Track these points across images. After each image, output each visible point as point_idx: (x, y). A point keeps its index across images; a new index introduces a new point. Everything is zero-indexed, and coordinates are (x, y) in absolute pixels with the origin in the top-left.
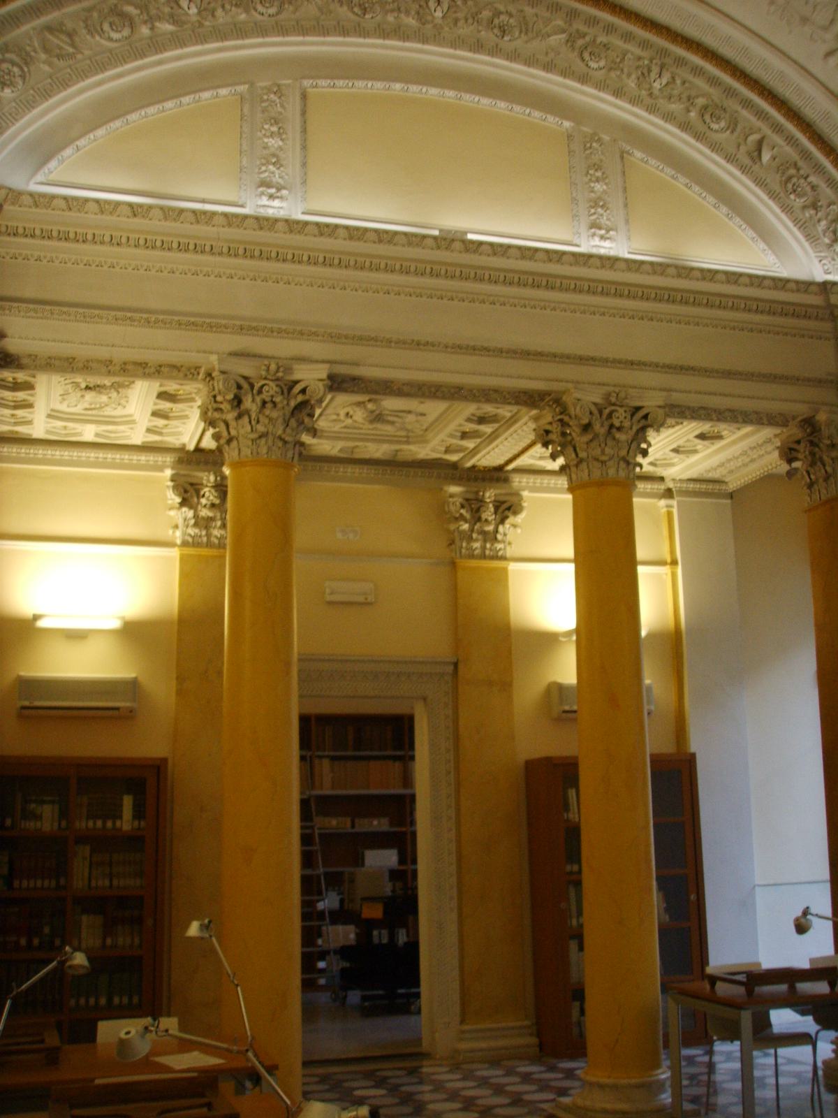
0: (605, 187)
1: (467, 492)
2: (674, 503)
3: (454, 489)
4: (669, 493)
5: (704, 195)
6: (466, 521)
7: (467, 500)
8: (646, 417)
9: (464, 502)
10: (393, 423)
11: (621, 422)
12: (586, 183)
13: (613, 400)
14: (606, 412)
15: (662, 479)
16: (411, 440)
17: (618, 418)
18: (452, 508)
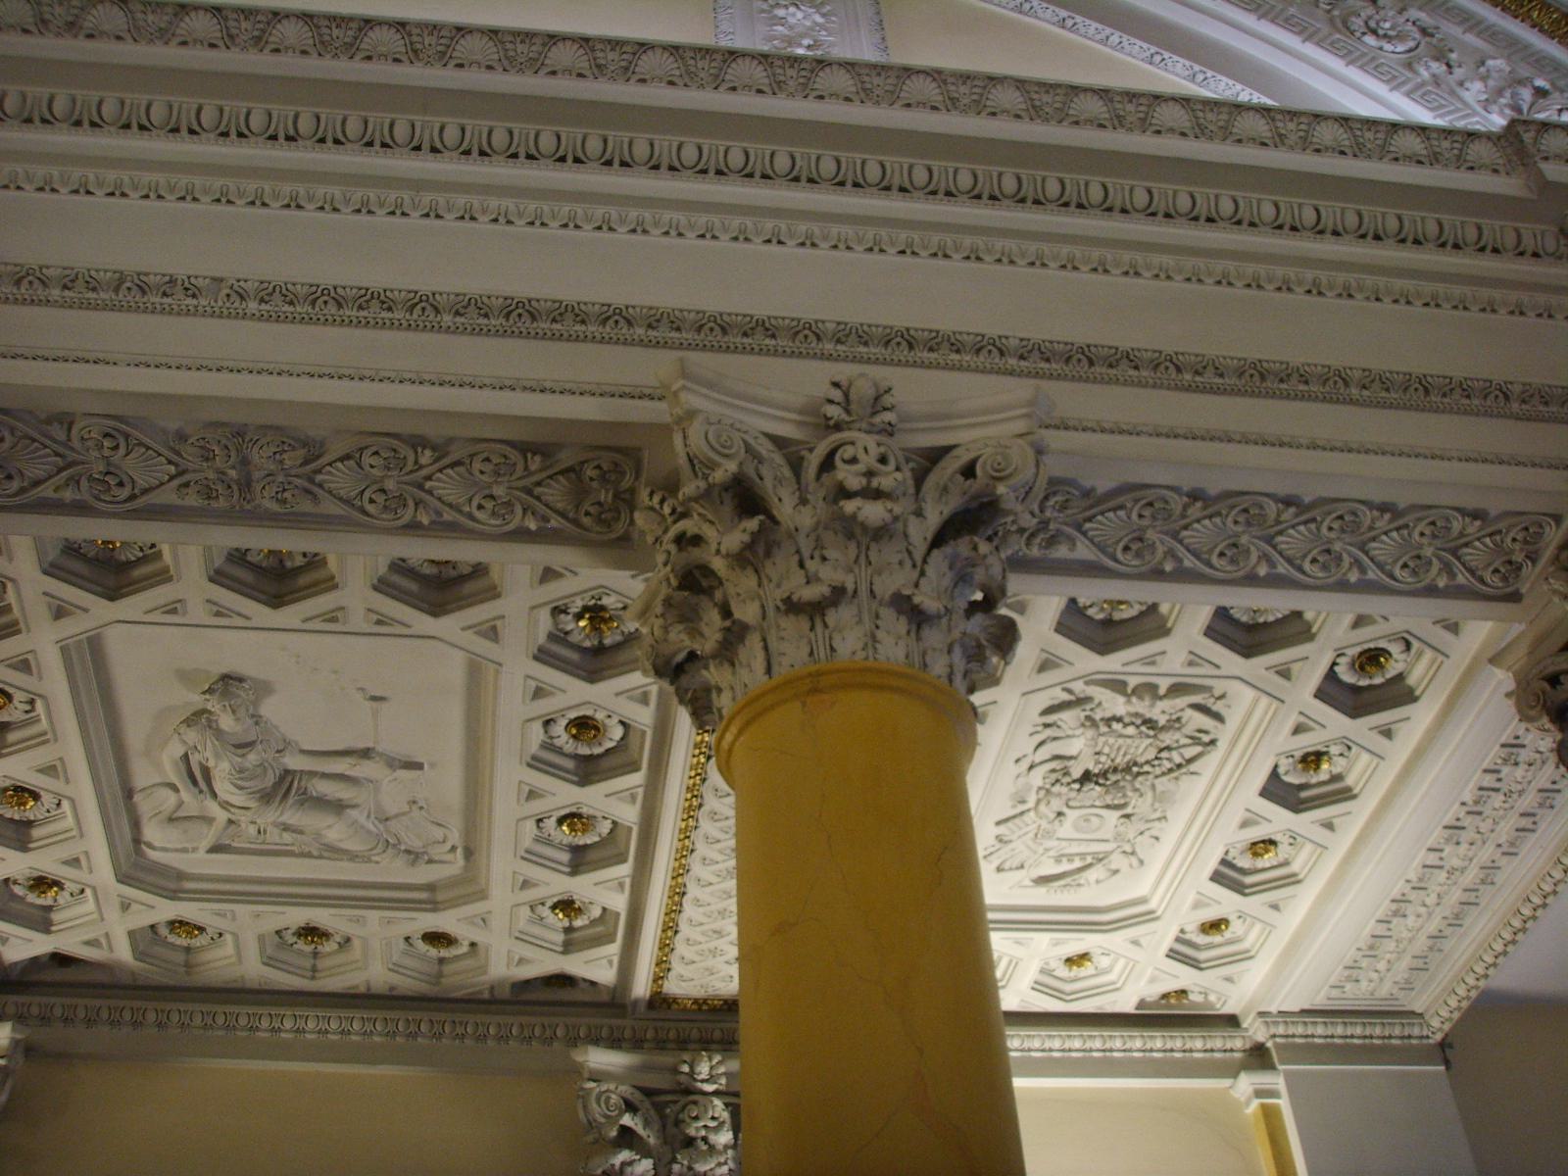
0: (819, 19)
1: (644, 1068)
2: (1277, 1081)
3: (600, 1058)
4: (1259, 1057)
5: (1115, 39)
6: (645, 1152)
7: (648, 1093)
8: (969, 471)
9: (637, 1097)
10: (339, 807)
11: (870, 474)
12: (763, 11)
13: (834, 412)
14: (814, 460)
15: (1232, 1021)
16: (440, 896)
17: (854, 460)
18: (597, 1111)
